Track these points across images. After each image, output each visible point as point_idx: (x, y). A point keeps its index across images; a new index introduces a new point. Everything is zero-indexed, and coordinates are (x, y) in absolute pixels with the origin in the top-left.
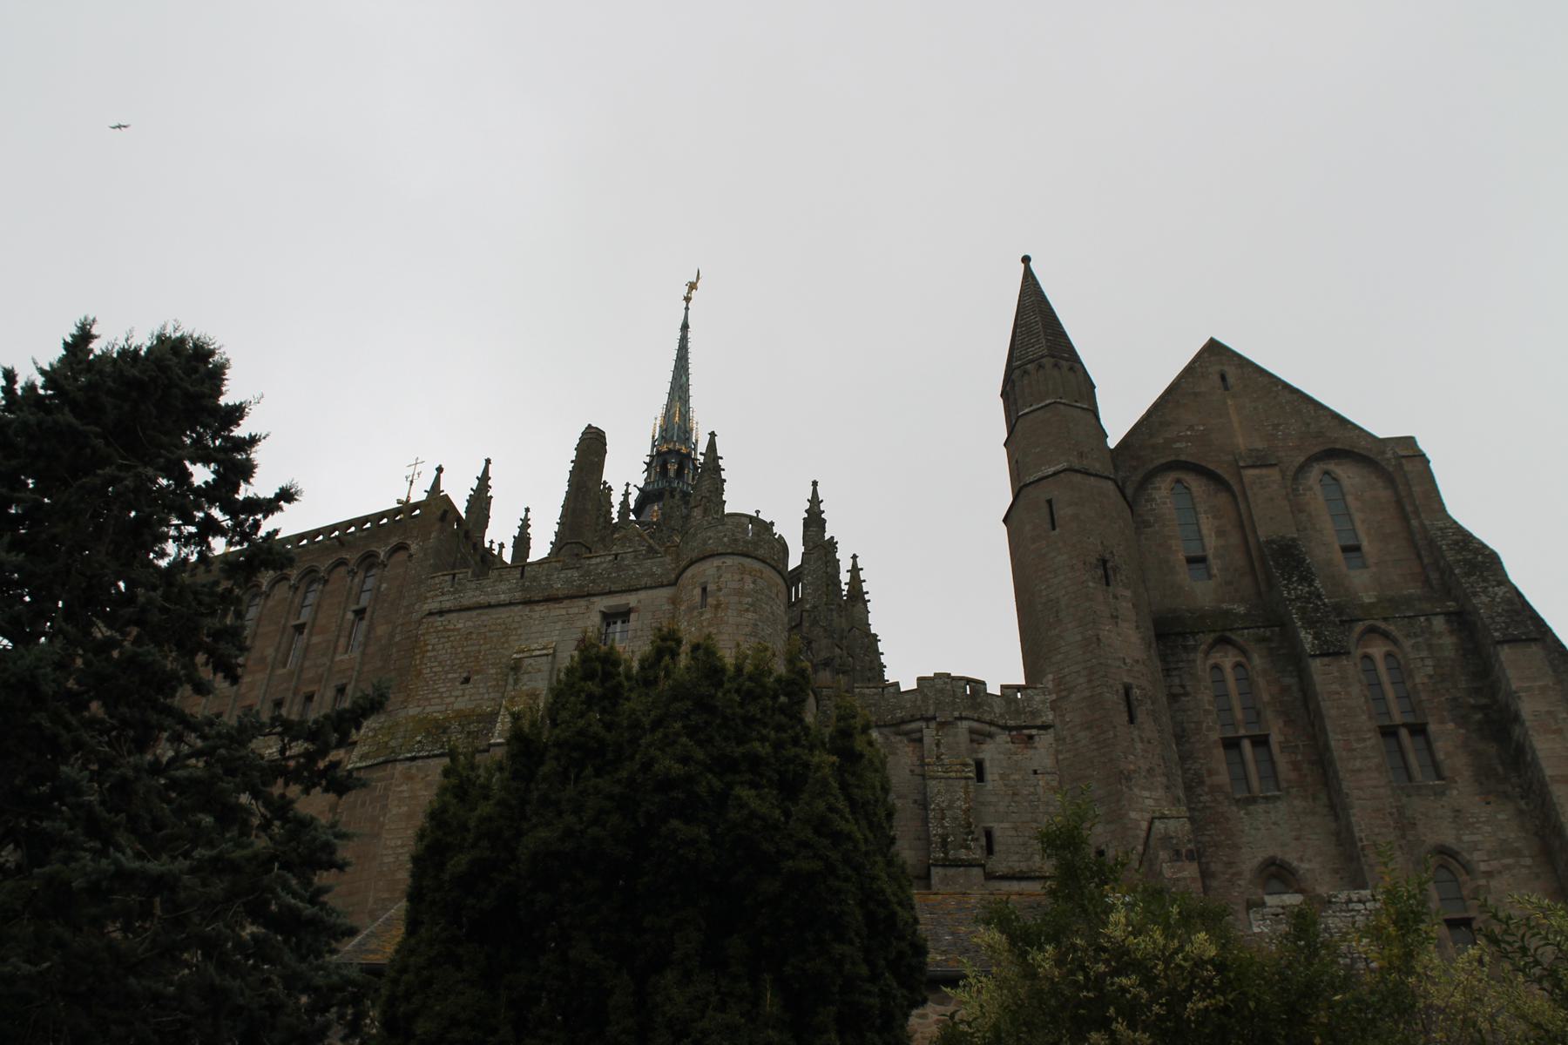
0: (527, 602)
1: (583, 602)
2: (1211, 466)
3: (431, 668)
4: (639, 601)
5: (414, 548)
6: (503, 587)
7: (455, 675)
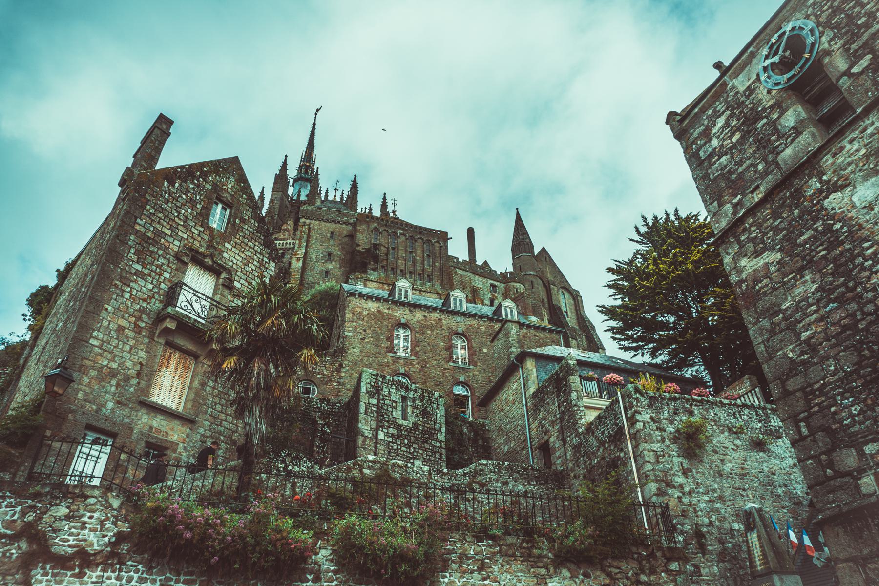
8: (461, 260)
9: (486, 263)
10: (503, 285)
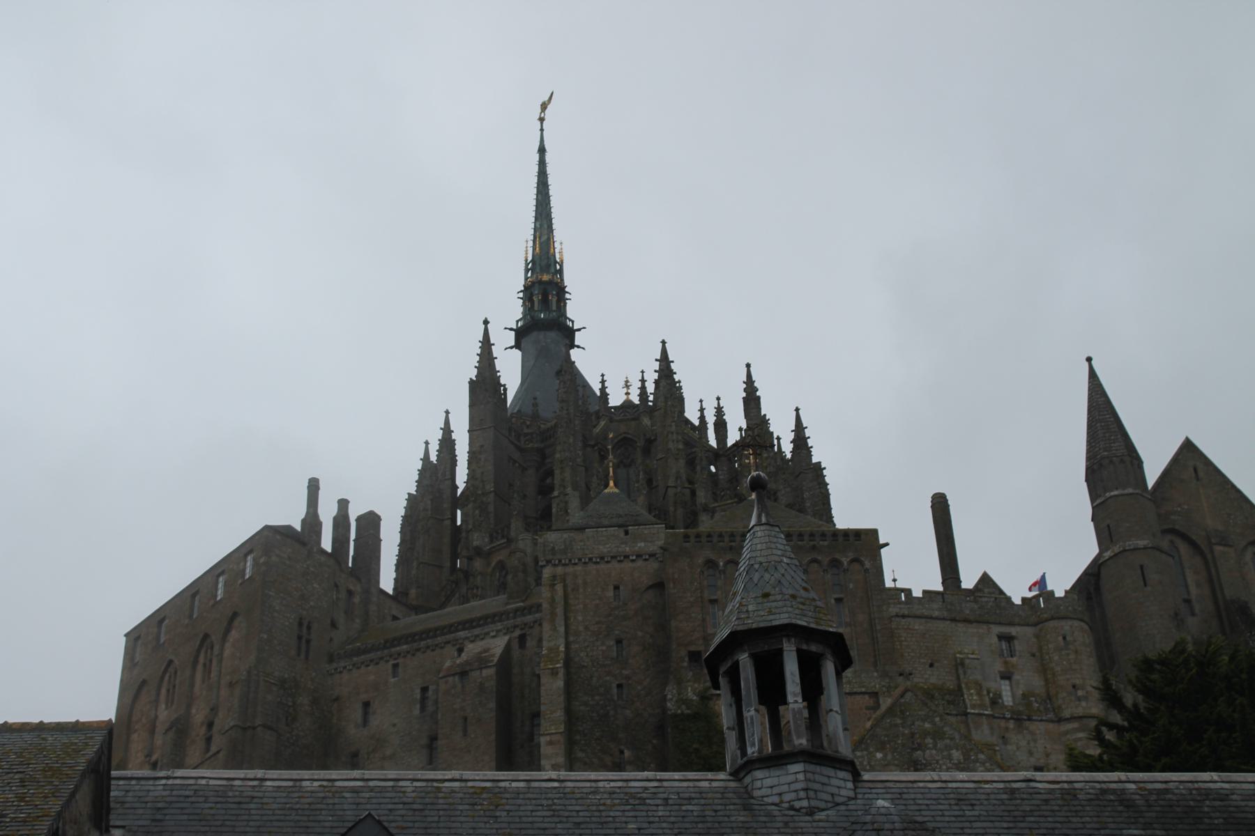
0: (953, 620)
1: (985, 627)
2: (1194, 538)
3: (909, 653)
4: (1017, 632)
5: (868, 564)
6: (935, 606)
7: (925, 661)
8: (917, 593)
9: (986, 580)
10: (1029, 631)
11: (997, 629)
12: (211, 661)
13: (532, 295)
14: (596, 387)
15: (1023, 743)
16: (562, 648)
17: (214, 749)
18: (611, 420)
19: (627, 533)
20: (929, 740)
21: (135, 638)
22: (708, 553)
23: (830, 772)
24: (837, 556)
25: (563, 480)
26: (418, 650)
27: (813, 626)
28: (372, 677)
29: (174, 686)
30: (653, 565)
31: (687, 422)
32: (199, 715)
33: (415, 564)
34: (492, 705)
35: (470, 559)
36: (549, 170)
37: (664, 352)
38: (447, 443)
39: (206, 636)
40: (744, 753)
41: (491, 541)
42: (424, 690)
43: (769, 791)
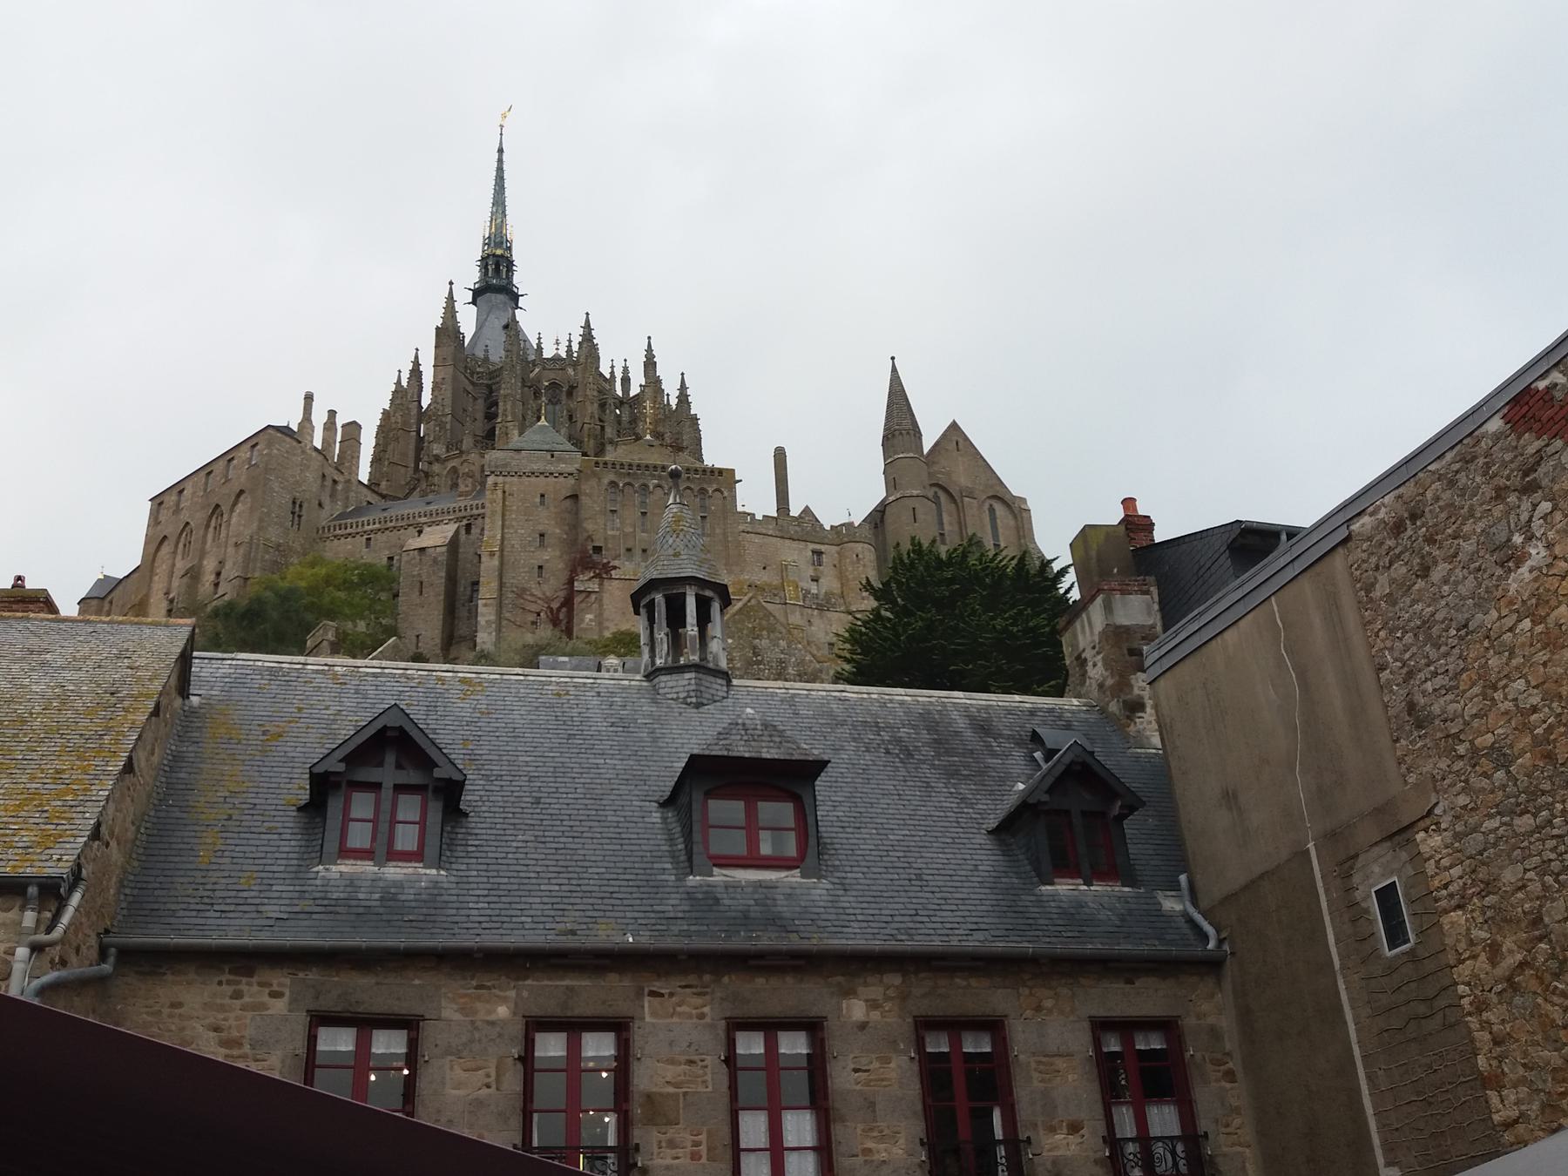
0: (782, 537)
1: (803, 543)
5: (726, 494)
8: (759, 517)
9: (807, 510)
11: (812, 546)
12: (220, 525)
13: (487, 264)
14: (534, 343)
15: (822, 626)
16: (499, 537)
17: (220, 592)
18: (544, 369)
19: (552, 456)
20: (765, 633)
21: (158, 501)
22: (612, 477)
23: (712, 679)
24: (705, 486)
25: (505, 410)
26: (387, 529)
27: (707, 578)
28: (350, 547)
29: (190, 542)
30: (571, 481)
31: (601, 375)
32: (210, 565)
33: (386, 463)
34: (443, 574)
35: (430, 463)
36: (505, 167)
37: (587, 321)
38: (416, 372)
39: (217, 506)
40: (653, 663)
41: (448, 451)
42: (391, 559)
43: (670, 690)
